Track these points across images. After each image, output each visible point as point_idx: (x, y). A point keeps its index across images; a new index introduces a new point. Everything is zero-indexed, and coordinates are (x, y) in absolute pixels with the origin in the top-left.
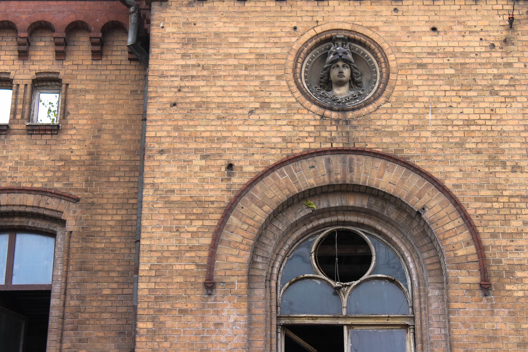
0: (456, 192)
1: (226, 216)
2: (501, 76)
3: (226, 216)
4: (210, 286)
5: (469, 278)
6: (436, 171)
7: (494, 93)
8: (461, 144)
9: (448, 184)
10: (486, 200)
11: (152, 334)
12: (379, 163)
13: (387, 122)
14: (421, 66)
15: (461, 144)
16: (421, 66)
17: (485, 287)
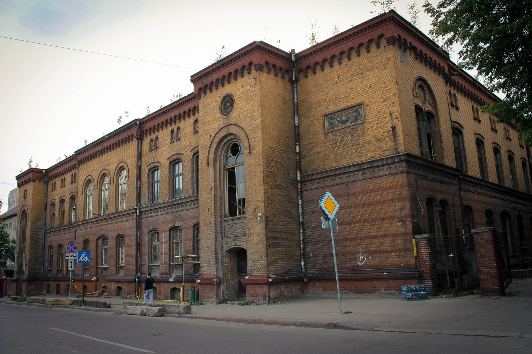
0: (245, 130)
1: (210, 148)
2: (253, 95)
3: (210, 148)
4: (208, 165)
5: (247, 151)
6: (242, 125)
7: (252, 100)
8: (246, 117)
9: (244, 128)
10: (250, 130)
11: (201, 178)
12: (233, 126)
13: (236, 114)
14: (240, 98)
15: (246, 117)
16: (240, 98)
17: (250, 153)
